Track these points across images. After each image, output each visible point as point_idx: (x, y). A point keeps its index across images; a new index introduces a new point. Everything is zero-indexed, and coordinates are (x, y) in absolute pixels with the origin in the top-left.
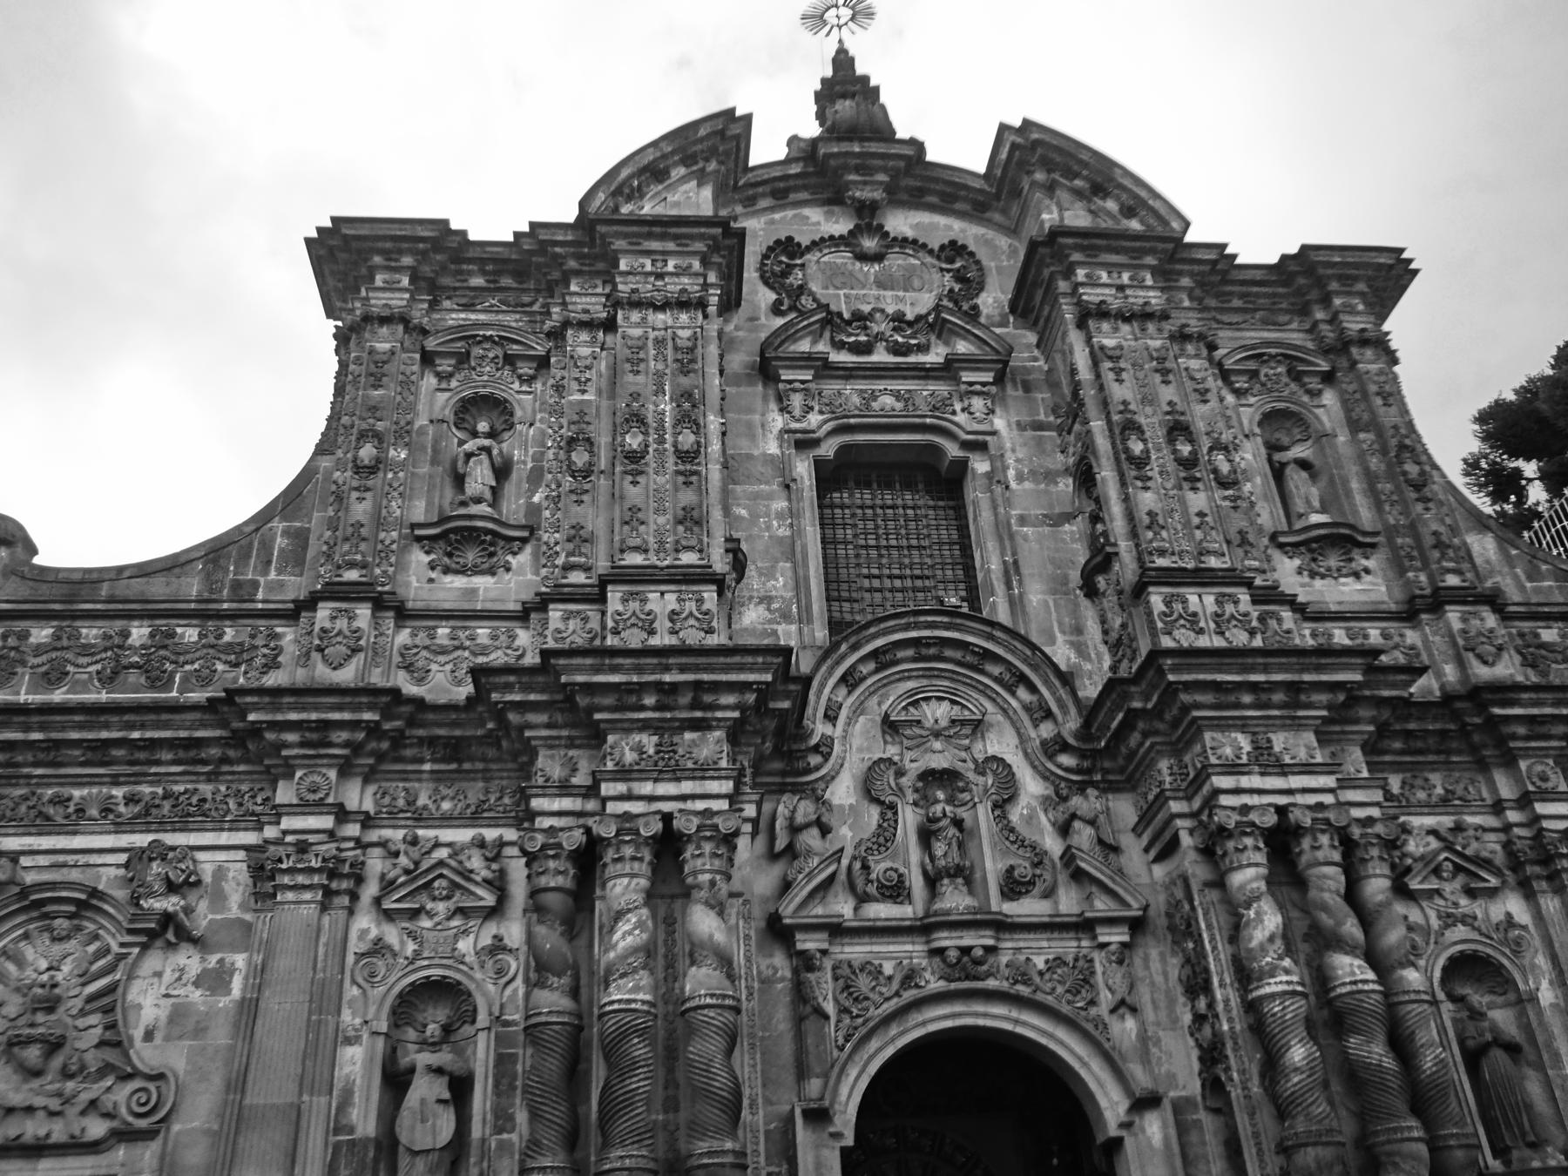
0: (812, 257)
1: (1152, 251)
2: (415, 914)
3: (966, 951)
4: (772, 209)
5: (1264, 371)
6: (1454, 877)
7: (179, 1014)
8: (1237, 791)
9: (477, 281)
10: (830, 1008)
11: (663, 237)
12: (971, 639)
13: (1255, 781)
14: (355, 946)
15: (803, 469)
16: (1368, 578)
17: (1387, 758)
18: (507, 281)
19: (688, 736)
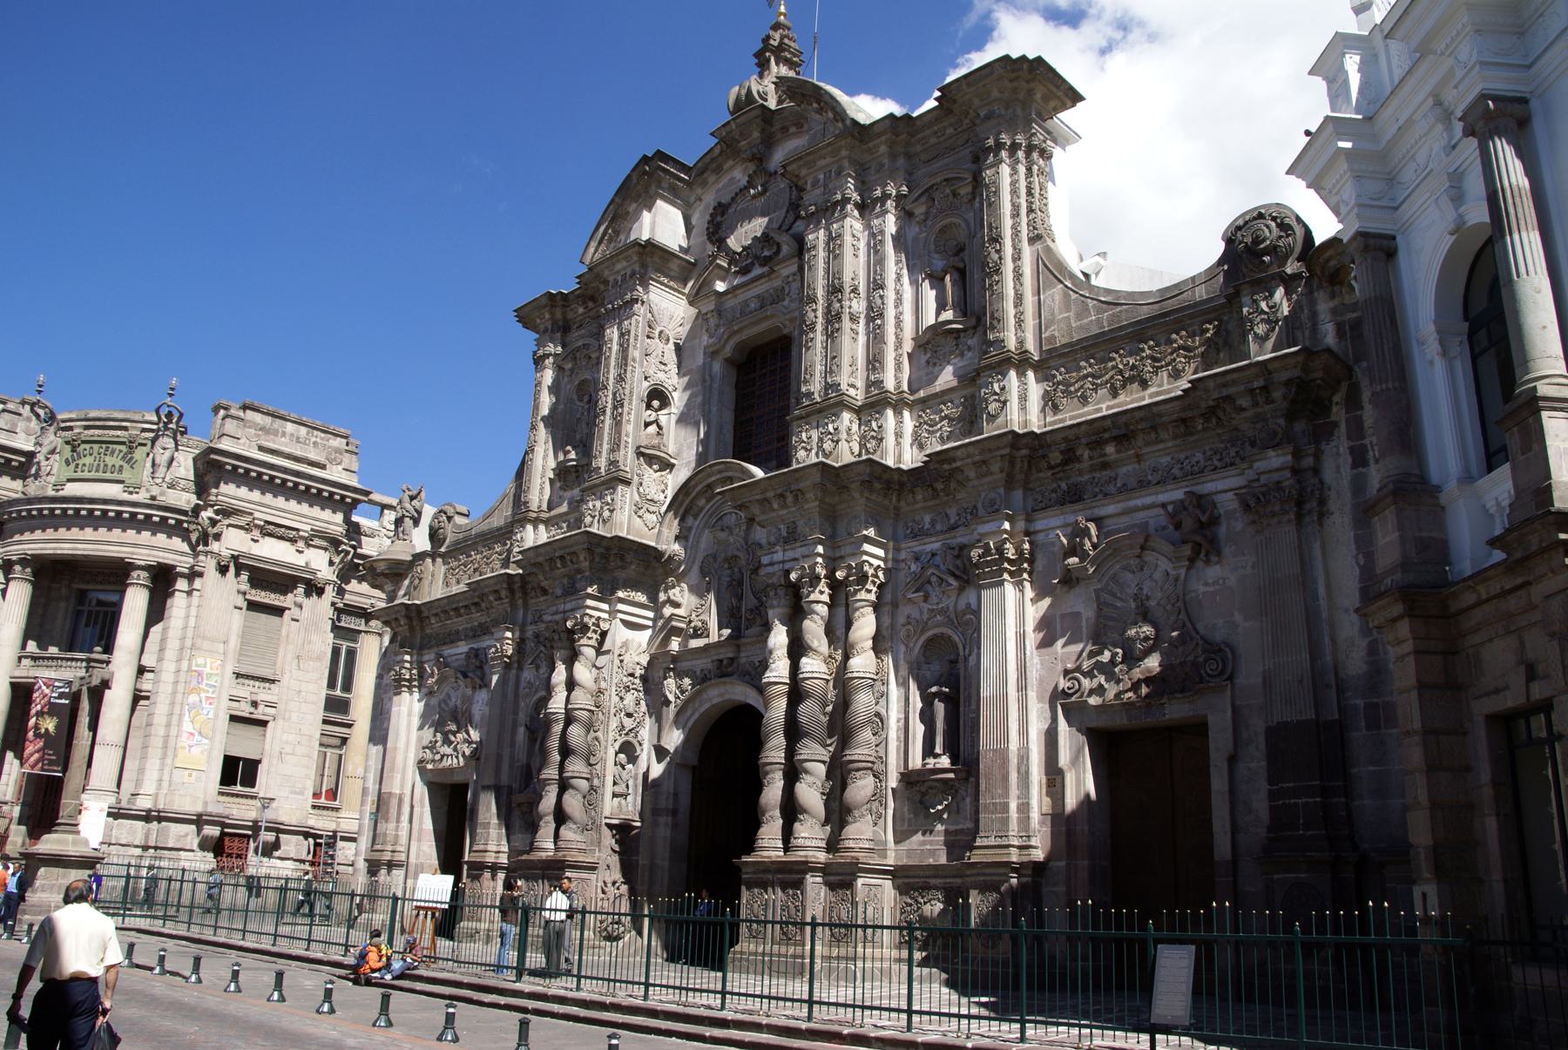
0: (731, 211)
1: (839, 149)
2: (538, 667)
3: (721, 661)
4: (717, 181)
5: (937, 196)
6: (940, 585)
7: (482, 718)
8: (771, 564)
9: (581, 310)
10: (671, 697)
11: (618, 261)
12: (700, 487)
13: (778, 556)
14: (523, 684)
15: (717, 367)
16: (970, 354)
17: (918, 506)
18: (591, 304)
19: (579, 576)
